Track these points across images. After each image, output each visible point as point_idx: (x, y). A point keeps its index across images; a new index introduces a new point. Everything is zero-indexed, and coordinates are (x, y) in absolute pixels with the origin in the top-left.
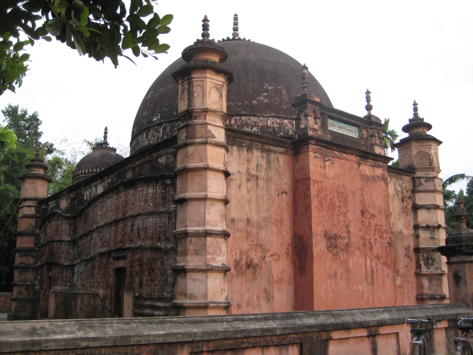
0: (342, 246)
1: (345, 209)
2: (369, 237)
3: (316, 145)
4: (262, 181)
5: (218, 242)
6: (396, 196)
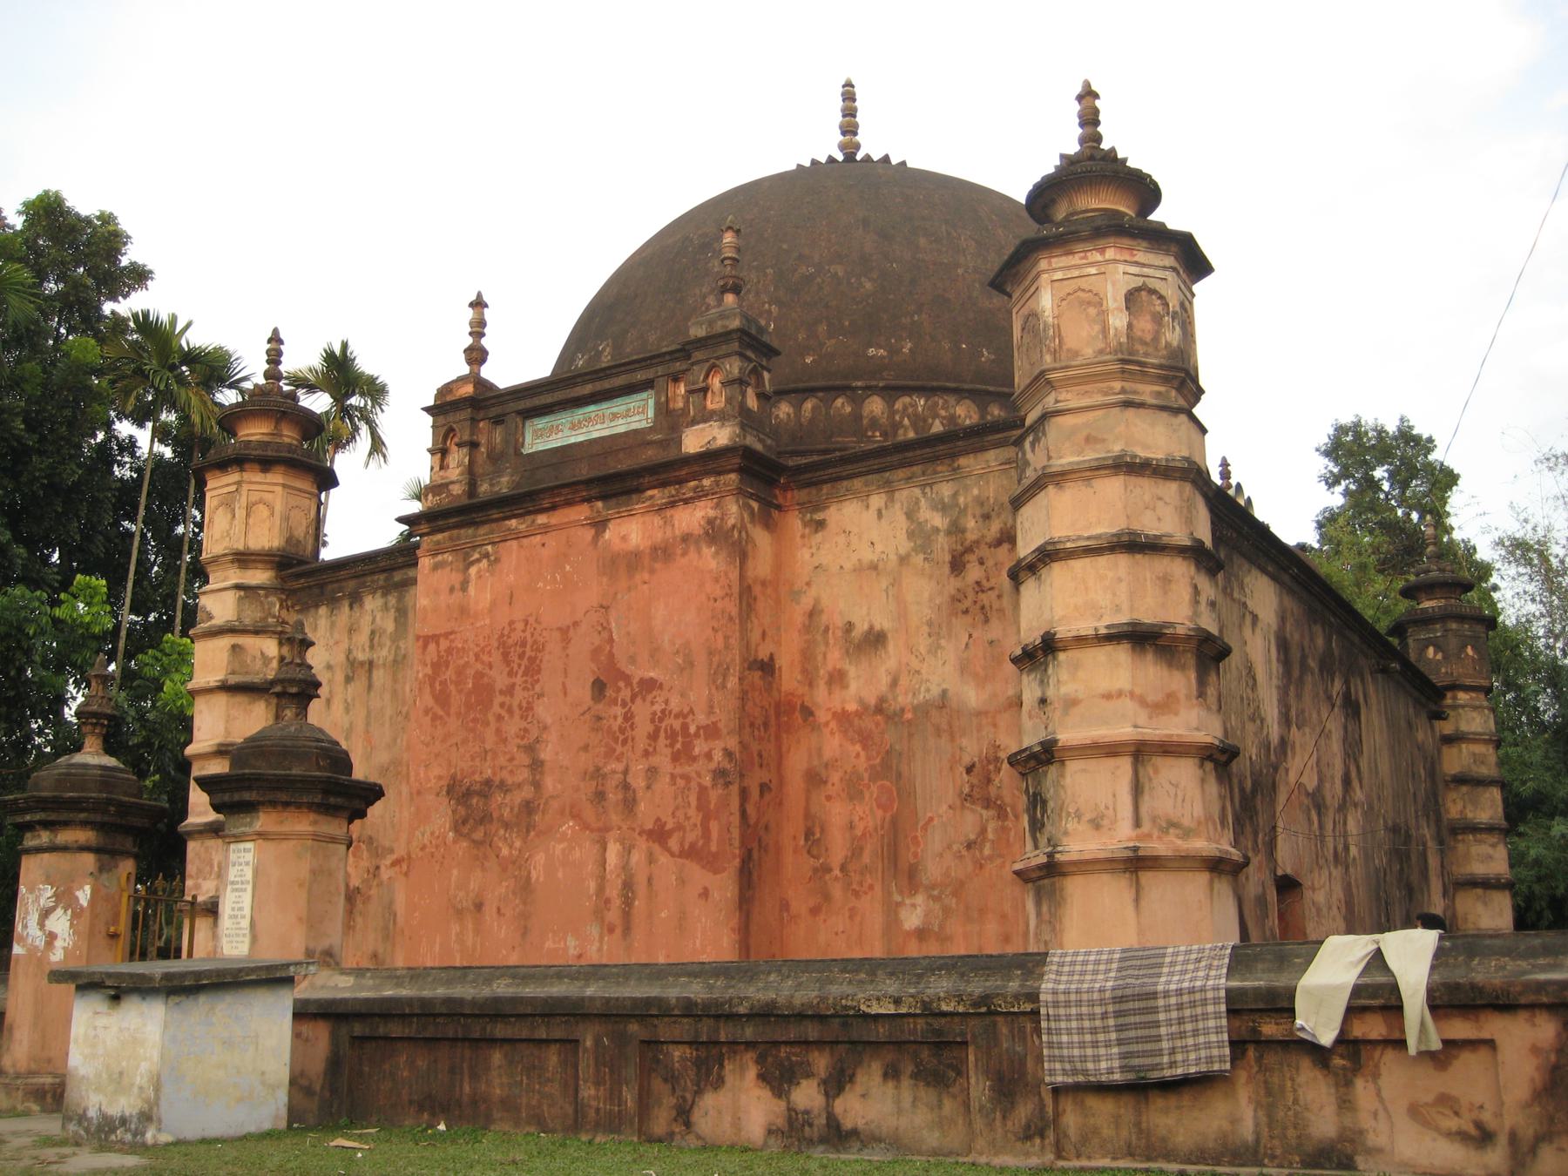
0: (506, 812)
1: (526, 694)
2: (620, 767)
3: (441, 531)
4: (381, 671)
5: (207, 849)
6: (918, 559)
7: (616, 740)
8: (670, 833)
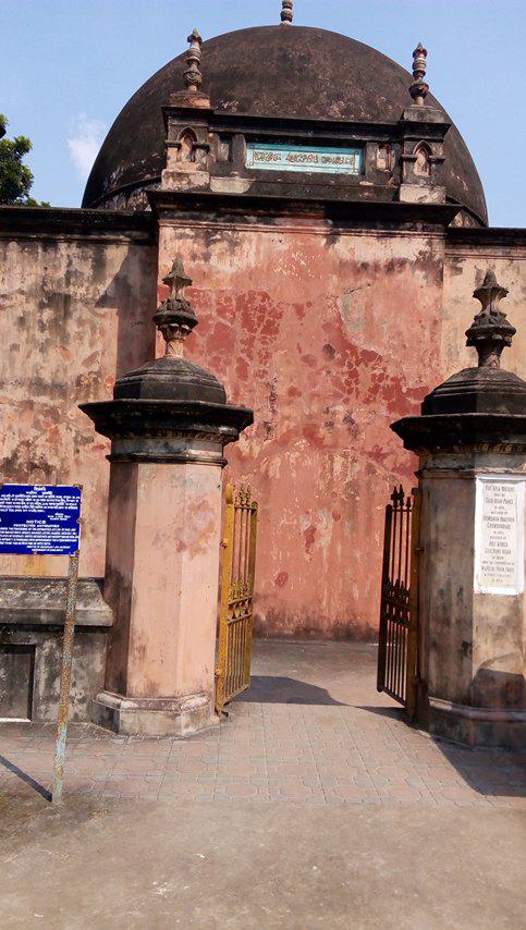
4: (79, 305)
7: (344, 390)
8: (385, 456)
